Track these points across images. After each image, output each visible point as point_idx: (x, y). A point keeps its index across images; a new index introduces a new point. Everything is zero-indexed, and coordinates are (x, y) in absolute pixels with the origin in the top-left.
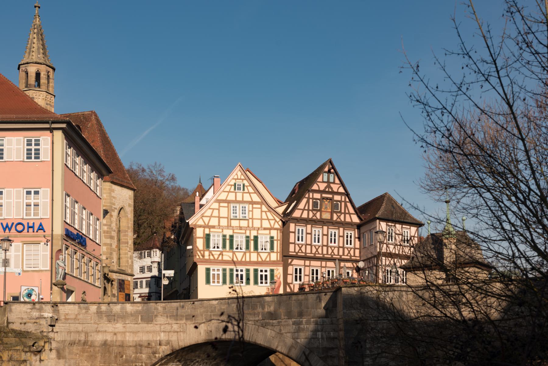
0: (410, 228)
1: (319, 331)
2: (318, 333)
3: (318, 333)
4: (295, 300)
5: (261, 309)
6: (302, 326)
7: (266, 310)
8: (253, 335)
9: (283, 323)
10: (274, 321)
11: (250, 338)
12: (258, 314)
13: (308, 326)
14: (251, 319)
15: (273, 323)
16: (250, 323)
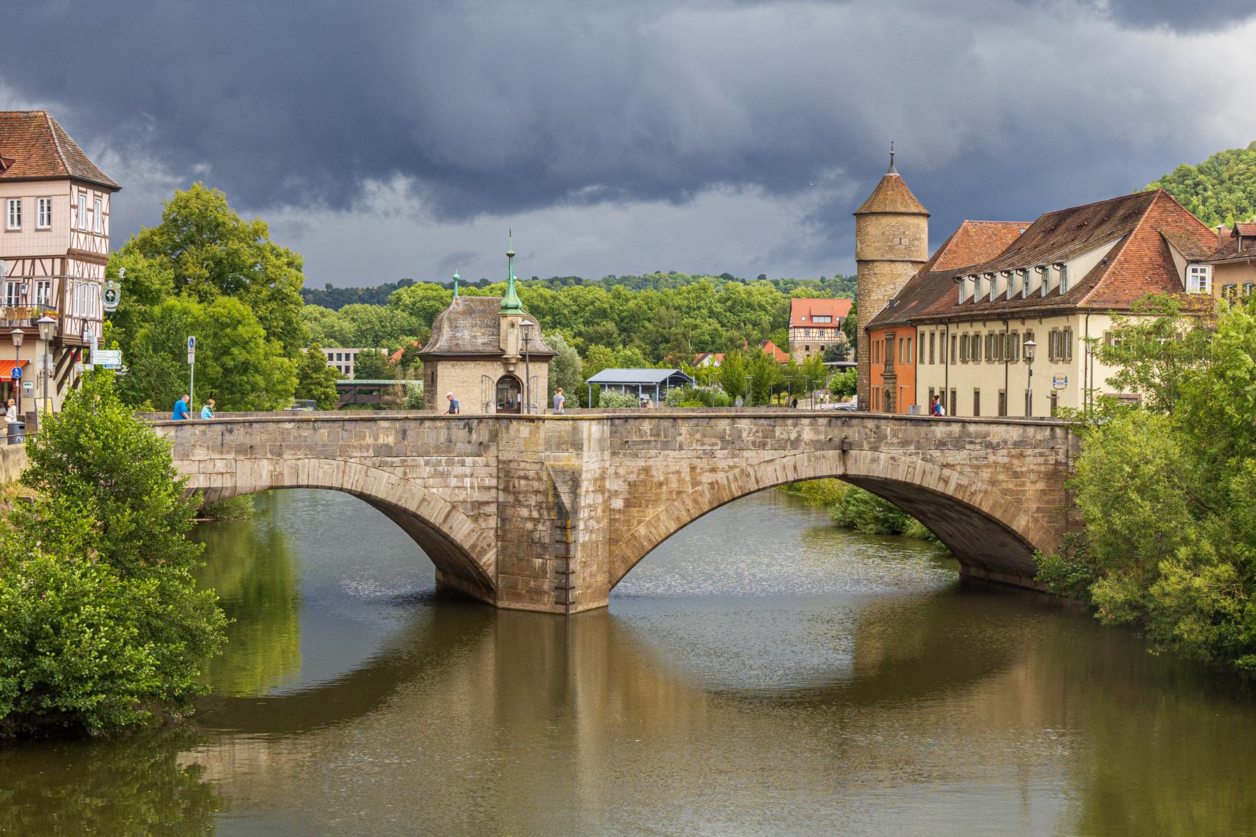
0: (86, 193)
1: (466, 476)
2: (465, 479)
3: (465, 479)
5: (372, 439)
6: (441, 469)
7: (381, 441)
8: (357, 481)
9: (409, 463)
10: (395, 459)
11: (352, 485)
12: (367, 447)
13: (450, 468)
14: (355, 454)
15: (393, 462)
16: (353, 460)
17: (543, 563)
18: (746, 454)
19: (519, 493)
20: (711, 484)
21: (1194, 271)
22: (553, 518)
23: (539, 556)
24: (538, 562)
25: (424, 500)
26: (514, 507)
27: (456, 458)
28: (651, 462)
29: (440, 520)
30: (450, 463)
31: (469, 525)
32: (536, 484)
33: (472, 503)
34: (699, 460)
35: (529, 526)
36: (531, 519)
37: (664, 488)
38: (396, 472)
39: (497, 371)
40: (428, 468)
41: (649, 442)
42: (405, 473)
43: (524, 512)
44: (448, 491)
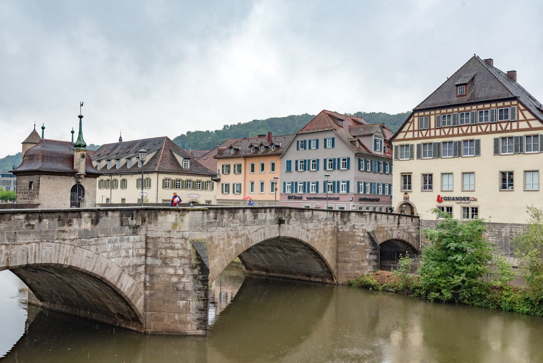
1: (130, 249)
3: (129, 251)
4: (111, 217)
6: (116, 245)
10: (91, 240)
13: (122, 243)
15: (90, 242)
17: (186, 304)
18: (249, 228)
19: (166, 258)
20: (236, 245)
21: (185, 161)
22: (195, 274)
23: (183, 299)
24: (182, 303)
25: (107, 267)
26: (161, 267)
27: (125, 237)
28: (213, 235)
29: (116, 279)
30: (122, 240)
31: (131, 281)
32: (181, 253)
33: (133, 266)
34: (231, 232)
35: (175, 279)
36: (176, 275)
37: (218, 248)
38: (92, 249)
39: (72, 182)
40: (110, 245)
41: (212, 223)
42: (97, 249)
43: (171, 271)
44: (121, 259)
